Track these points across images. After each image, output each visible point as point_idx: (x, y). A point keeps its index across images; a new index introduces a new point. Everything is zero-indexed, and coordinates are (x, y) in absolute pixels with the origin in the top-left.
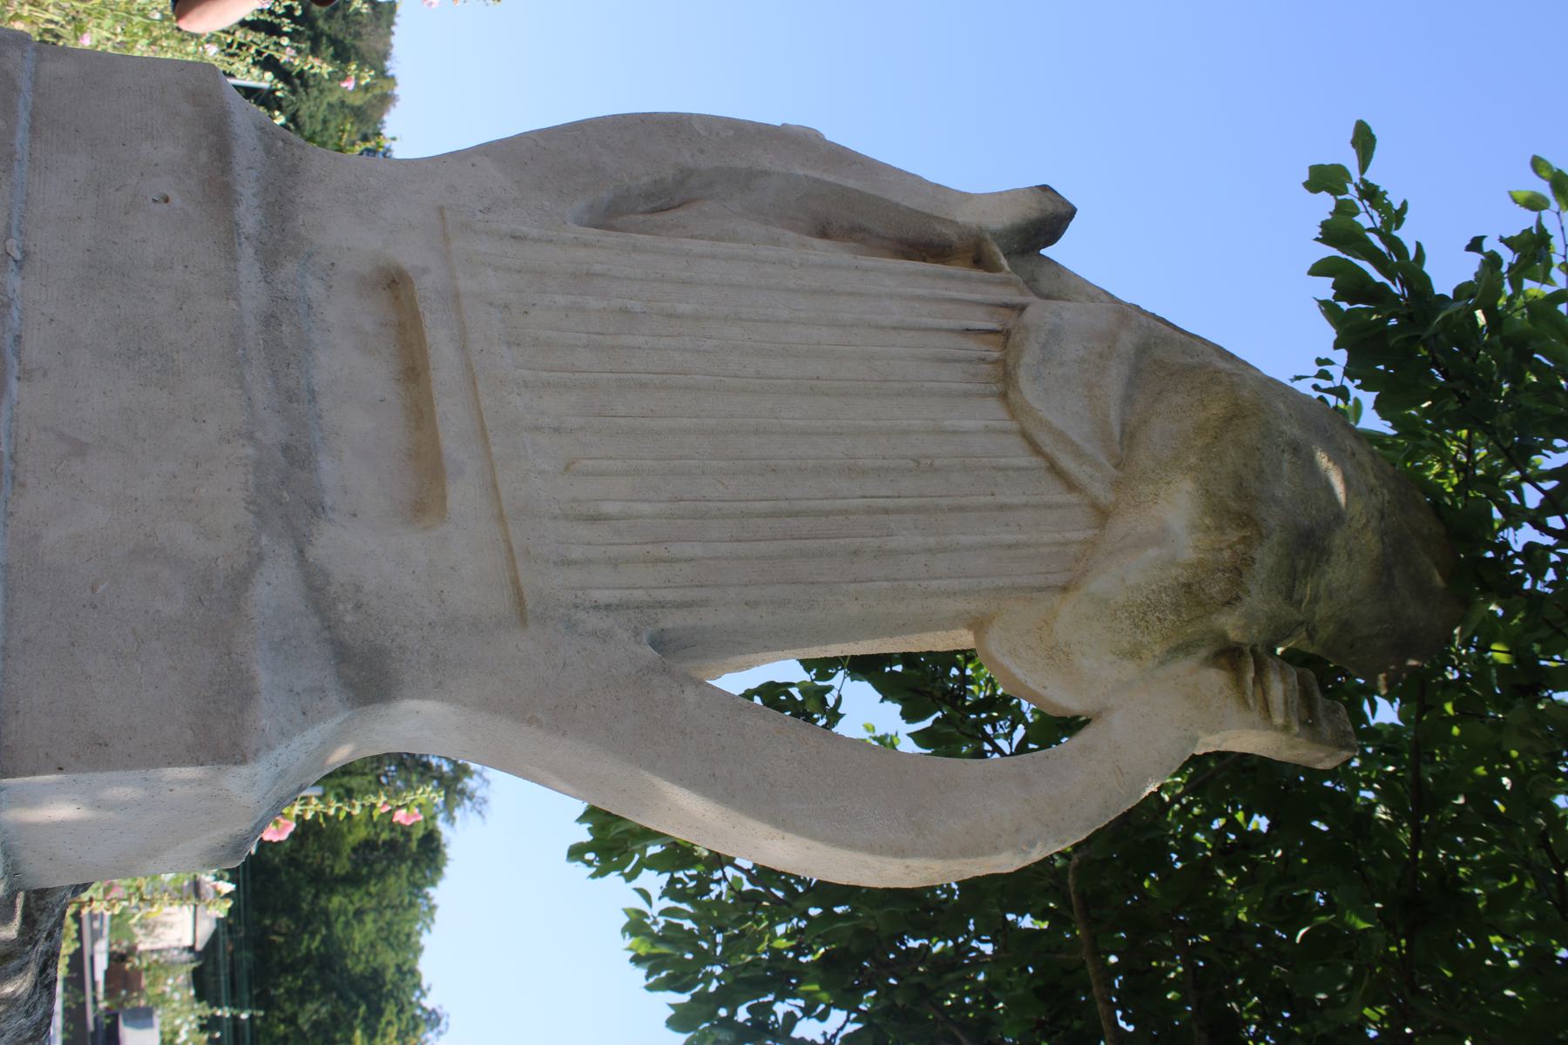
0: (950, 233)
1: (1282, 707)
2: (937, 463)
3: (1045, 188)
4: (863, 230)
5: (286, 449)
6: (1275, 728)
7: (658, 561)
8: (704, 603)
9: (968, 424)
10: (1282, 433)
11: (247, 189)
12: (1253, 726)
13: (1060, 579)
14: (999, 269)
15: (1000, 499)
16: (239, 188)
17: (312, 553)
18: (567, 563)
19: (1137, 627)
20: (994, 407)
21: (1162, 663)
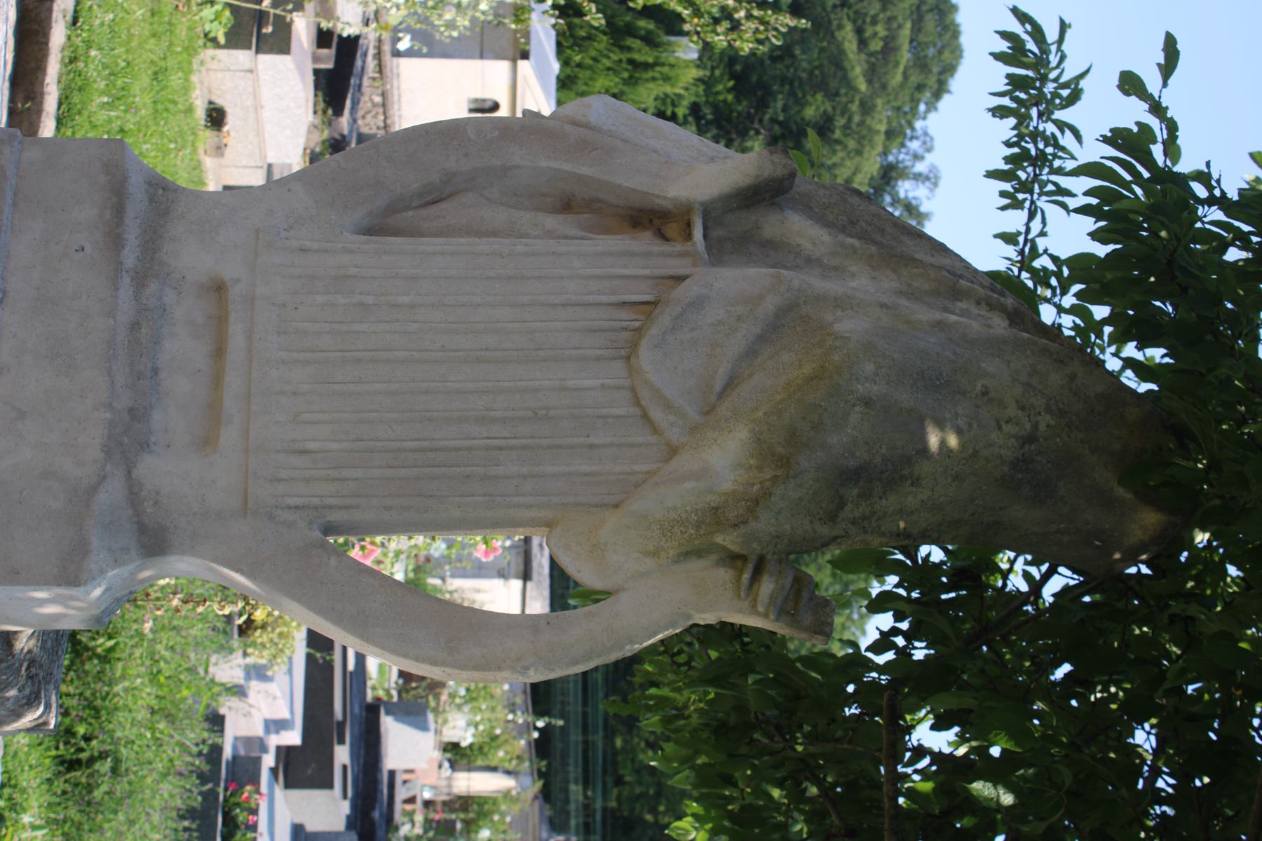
0: (666, 204)
1: (766, 601)
2: (552, 413)
4: (599, 201)
5: (131, 411)
7: (334, 479)
8: (357, 507)
9: (588, 383)
12: (740, 611)
16: (126, 236)
17: (135, 473)
18: (280, 480)
19: (664, 535)
20: (618, 367)
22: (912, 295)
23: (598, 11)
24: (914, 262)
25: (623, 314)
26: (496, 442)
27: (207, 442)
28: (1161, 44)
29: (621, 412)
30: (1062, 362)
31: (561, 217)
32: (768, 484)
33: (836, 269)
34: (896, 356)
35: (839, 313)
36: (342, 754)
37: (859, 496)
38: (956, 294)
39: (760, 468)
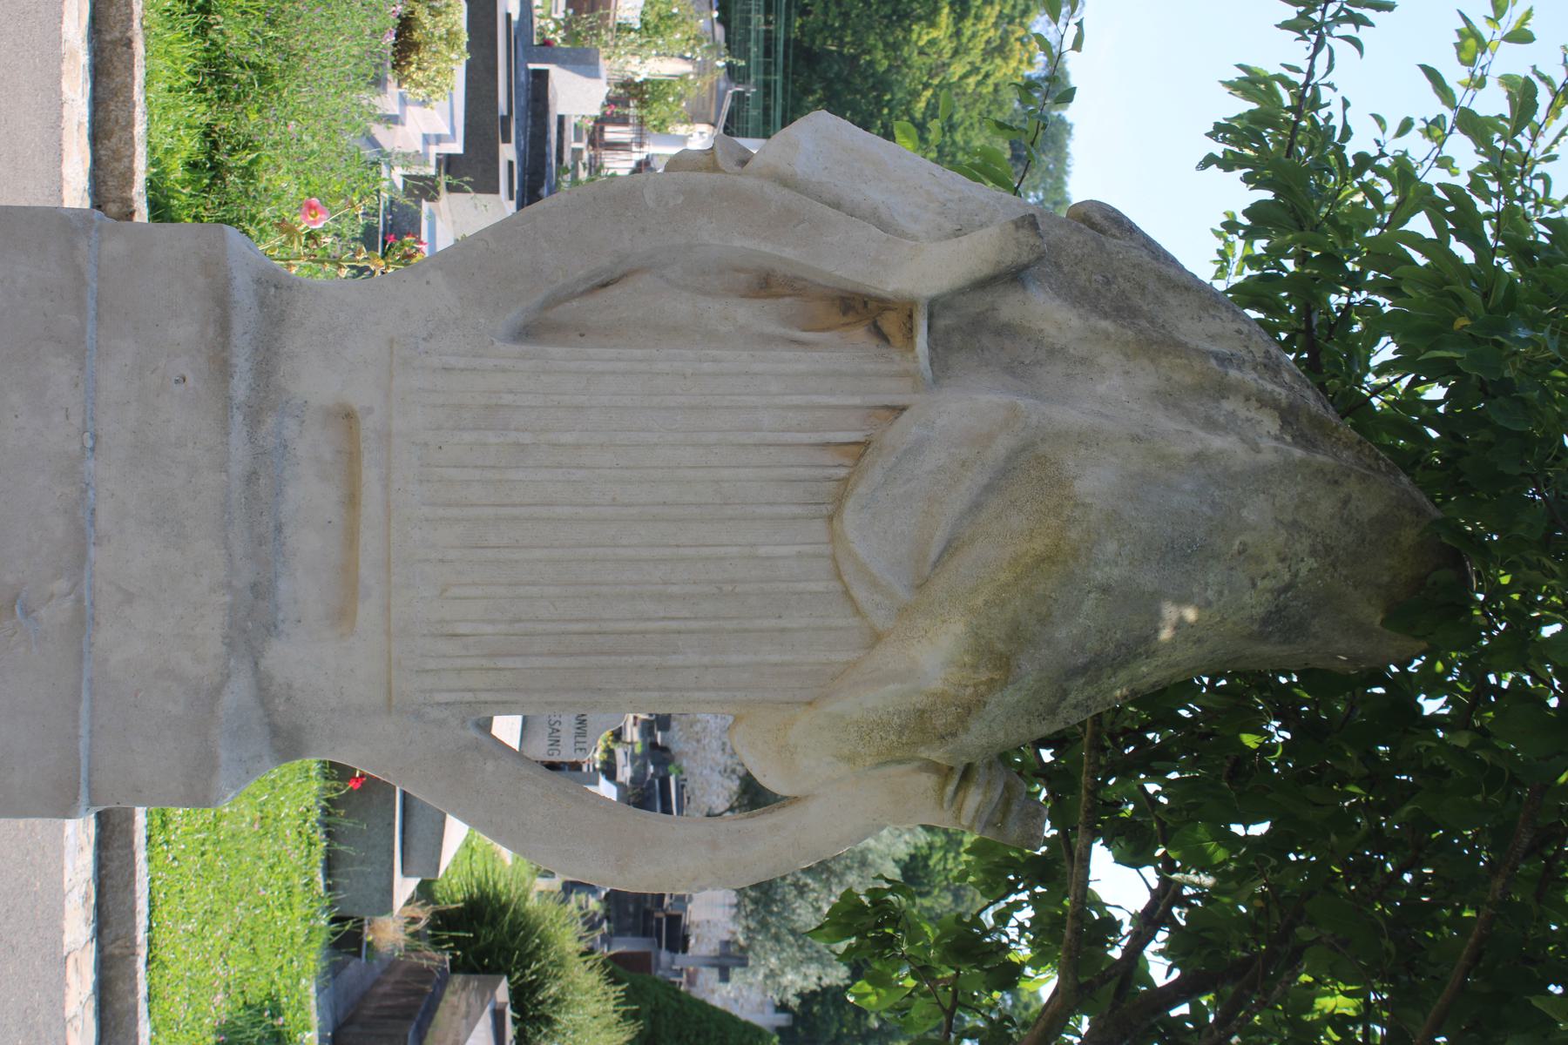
0: (884, 295)
4: (803, 279)
11: (242, 360)
14: (913, 349)
15: (783, 623)
16: (234, 361)
17: (263, 664)
19: (862, 739)
22: (1167, 398)
24: (1179, 348)
25: (828, 457)
26: (674, 625)
27: (343, 615)
29: (819, 587)
30: (1336, 482)
31: (757, 303)
32: (983, 688)
33: (1083, 361)
34: (1144, 525)
35: (1082, 452)
36: (508, 152)
37: (1086, 683)
38: (1223, 390)
39: (975, 667)
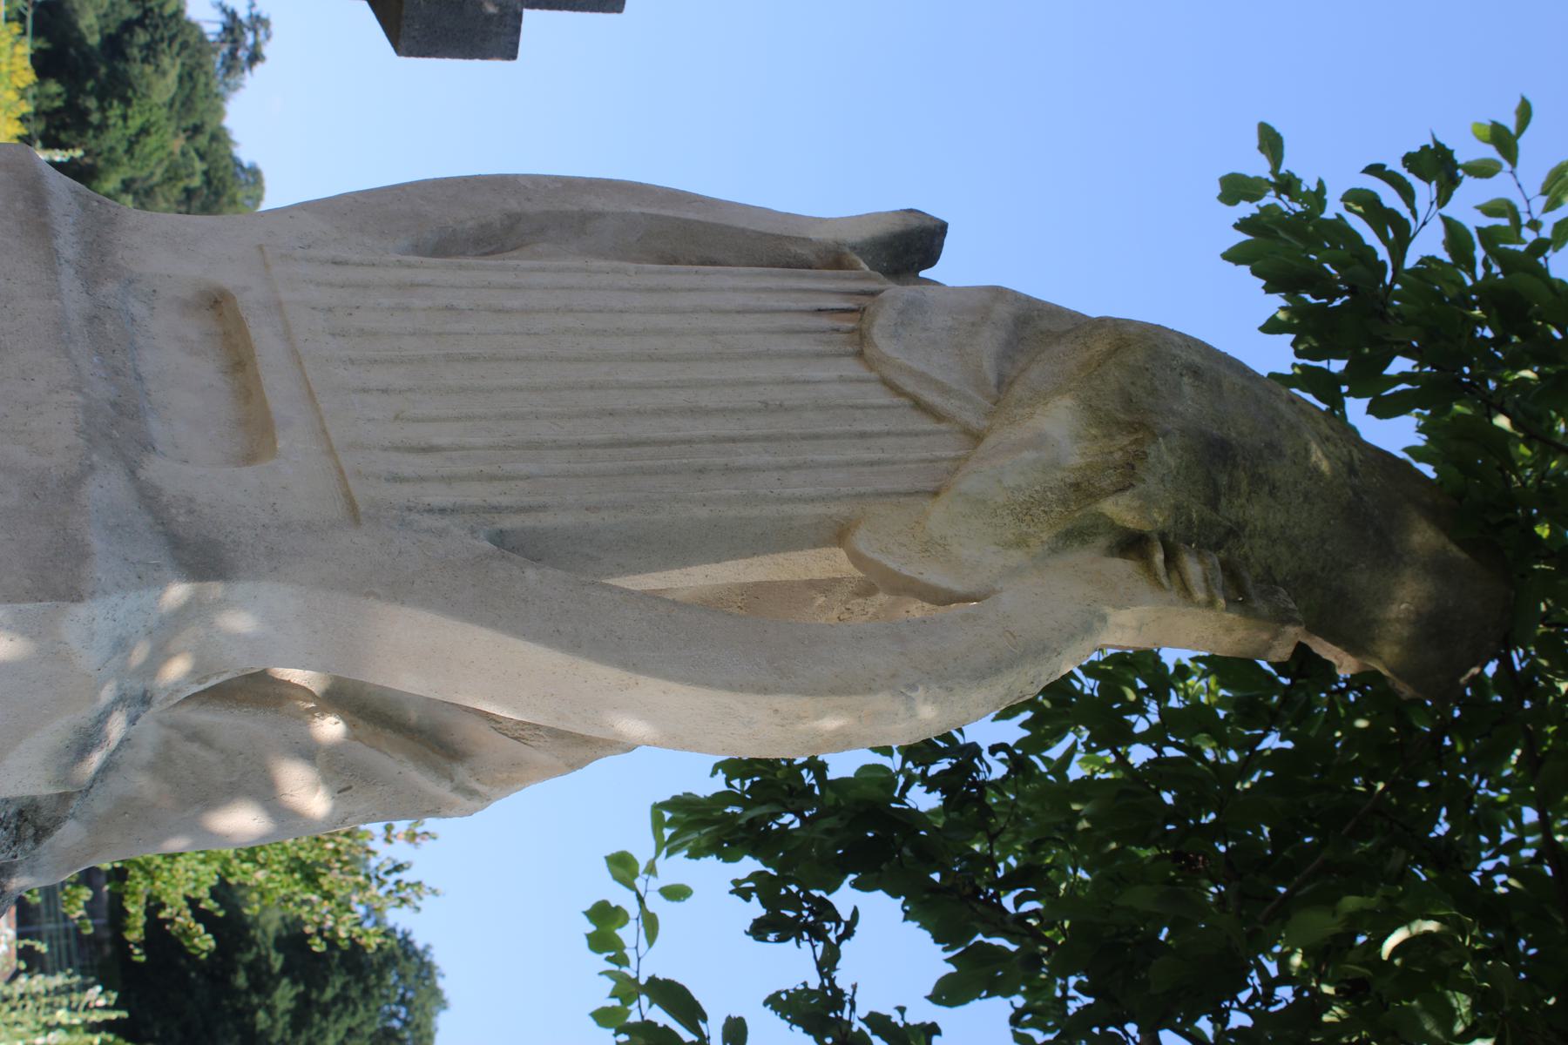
1: (1203, 585)
3: (911, 211)
6: (1198, 604)
8: (544, 508)
10: (1175, 357)
12: (1171, 603)
13: (930, 486)
15: (858, 427)
17: (142, 474)
21: (1054, 551)
23: (207, 932)
28: (1254, 140)
39: (1111, 436)
